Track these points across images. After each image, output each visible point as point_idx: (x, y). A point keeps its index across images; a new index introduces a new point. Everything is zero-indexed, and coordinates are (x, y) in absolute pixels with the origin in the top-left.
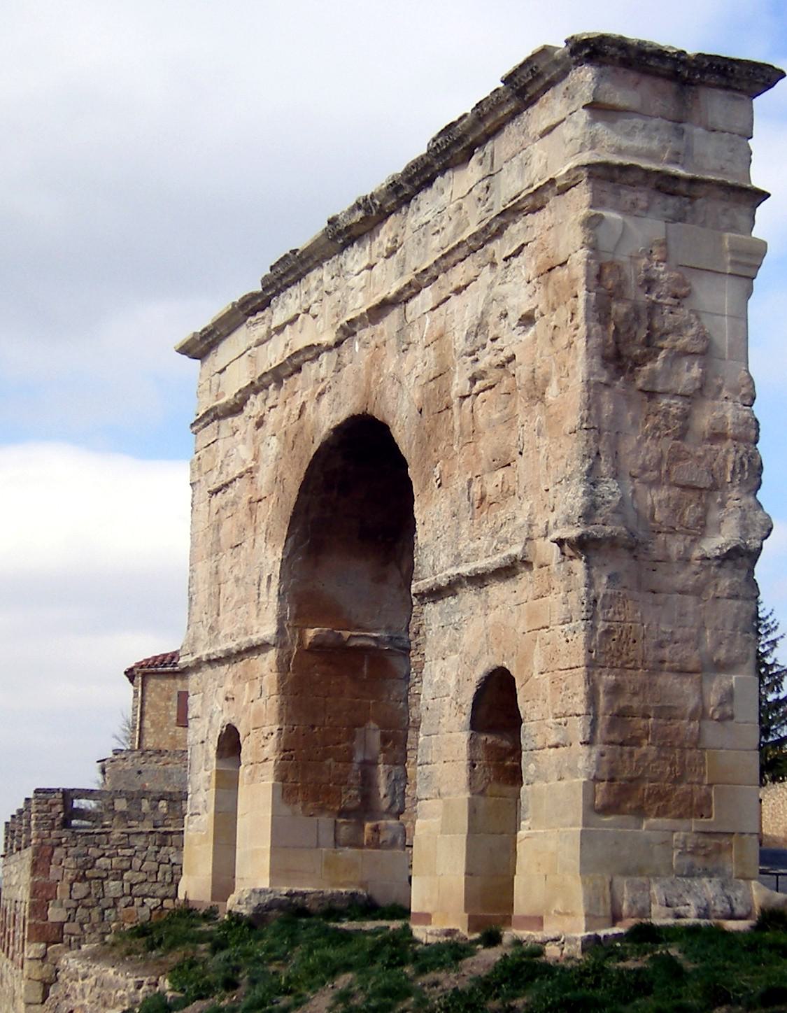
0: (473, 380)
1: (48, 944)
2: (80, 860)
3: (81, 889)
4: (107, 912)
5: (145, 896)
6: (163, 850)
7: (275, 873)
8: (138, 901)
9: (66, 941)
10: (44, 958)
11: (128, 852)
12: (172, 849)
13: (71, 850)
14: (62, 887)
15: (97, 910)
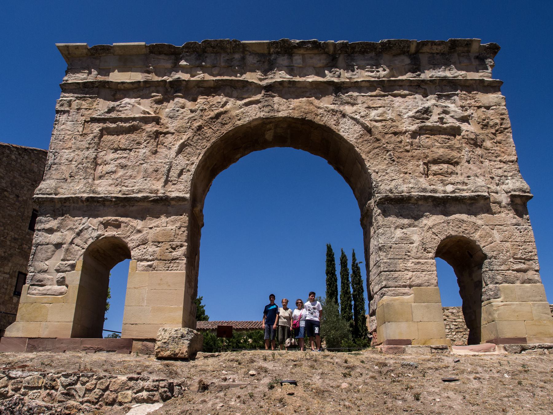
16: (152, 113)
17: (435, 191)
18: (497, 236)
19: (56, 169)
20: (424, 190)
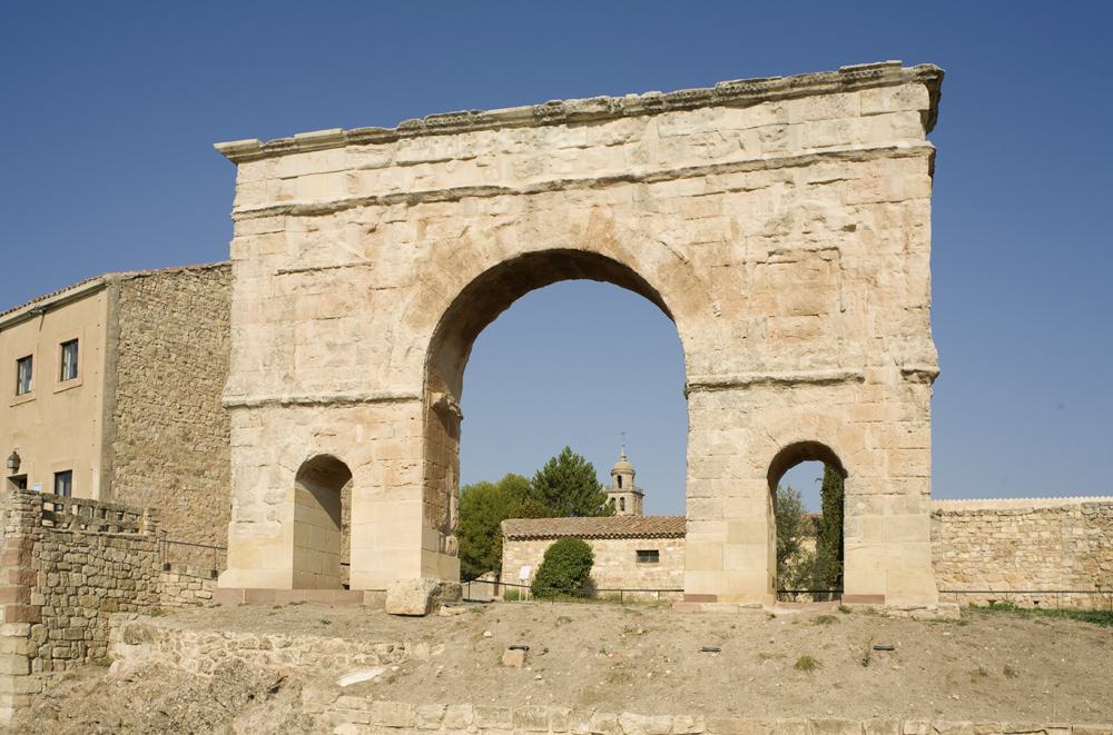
0: (771, 254)
1: (33, 623)
2: (53, 554)
3: (54, 578)
4: (71, 598)
5: (96, 587)
6: (108, 549)
7: (425, 568)
8: (92, 591)
9: (44, 622)
10: (29, 636)
11: (85, 550)
12: (114, 550)
13: (47, 545)
14: (40, 577)
15: (65, 596)
17: (780, 367)
18: (869, 440)
19: (245, 356)
20: (761, 366)
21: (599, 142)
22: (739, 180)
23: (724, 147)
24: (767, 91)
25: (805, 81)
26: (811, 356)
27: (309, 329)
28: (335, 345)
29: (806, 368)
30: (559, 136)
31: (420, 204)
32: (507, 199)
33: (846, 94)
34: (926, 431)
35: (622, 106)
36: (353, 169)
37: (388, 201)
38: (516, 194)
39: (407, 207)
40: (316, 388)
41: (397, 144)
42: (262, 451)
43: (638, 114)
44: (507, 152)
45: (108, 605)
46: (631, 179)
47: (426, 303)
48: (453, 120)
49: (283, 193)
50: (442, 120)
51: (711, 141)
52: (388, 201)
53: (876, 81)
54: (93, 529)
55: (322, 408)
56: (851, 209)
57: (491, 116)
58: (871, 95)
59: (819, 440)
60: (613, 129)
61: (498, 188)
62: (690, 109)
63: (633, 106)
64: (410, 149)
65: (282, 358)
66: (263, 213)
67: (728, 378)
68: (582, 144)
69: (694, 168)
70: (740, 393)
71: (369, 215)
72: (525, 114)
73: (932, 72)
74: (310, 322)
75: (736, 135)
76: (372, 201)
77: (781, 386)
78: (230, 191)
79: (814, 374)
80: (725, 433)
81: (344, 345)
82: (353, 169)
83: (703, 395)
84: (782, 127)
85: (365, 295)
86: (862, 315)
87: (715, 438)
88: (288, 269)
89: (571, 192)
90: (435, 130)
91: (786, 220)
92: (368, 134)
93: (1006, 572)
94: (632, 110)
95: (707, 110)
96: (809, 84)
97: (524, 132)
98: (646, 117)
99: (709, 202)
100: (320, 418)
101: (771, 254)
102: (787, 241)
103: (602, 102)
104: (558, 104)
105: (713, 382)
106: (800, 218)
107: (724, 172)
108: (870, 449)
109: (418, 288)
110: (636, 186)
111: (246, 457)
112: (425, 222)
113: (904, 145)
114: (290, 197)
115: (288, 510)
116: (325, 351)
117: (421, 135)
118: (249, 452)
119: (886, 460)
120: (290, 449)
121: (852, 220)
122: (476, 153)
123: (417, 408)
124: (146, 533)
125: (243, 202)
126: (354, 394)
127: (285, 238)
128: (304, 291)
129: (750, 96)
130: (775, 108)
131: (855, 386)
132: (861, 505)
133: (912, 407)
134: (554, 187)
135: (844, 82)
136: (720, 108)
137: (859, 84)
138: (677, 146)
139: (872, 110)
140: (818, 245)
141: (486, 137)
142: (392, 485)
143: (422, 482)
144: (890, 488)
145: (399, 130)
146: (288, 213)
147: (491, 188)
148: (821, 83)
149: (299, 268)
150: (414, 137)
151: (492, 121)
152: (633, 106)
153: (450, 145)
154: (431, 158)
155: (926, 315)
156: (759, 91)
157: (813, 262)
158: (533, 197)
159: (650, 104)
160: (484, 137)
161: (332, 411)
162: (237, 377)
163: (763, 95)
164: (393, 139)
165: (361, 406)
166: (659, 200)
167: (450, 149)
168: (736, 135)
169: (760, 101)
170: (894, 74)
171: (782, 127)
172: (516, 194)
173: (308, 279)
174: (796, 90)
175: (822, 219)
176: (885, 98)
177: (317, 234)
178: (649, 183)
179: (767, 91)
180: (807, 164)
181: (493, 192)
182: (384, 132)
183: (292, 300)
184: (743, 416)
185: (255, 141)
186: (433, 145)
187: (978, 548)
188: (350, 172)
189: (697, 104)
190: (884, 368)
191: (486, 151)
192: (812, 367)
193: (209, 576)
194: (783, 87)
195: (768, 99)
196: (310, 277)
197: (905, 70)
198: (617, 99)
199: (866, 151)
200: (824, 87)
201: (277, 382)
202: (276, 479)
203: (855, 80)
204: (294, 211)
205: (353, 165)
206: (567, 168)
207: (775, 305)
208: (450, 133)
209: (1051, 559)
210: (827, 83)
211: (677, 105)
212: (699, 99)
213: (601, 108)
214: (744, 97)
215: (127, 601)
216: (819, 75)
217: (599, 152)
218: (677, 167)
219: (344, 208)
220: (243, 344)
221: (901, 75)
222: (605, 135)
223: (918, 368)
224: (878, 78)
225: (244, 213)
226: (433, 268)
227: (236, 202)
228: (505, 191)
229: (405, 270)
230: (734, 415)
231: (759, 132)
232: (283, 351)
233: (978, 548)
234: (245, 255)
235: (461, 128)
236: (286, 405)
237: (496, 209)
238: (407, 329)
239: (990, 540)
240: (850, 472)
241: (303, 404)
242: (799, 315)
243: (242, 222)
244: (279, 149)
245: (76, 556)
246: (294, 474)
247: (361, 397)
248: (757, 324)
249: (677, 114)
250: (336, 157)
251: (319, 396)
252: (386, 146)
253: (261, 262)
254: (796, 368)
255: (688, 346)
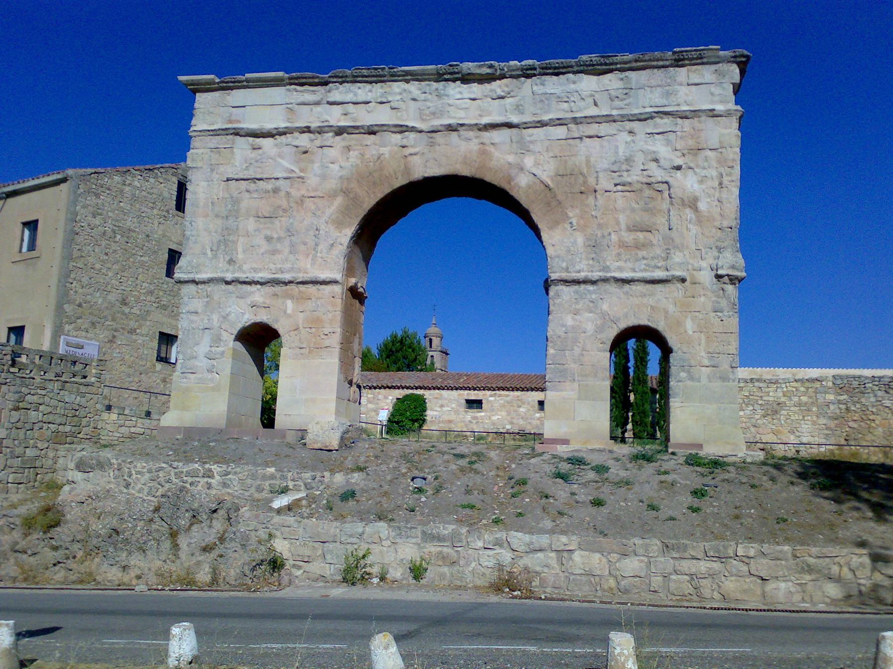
0: (616, 185)
2: (17, 396)
6: (62, 393)
7: (338, 413)
9: (4, 452)
11: (43, 392)
12: (66, 393)
13: (12, 388)
15: (23, 431)
16: (297, 170)
17: (620, 269)
18: (689, 326)
19: (196, 242)
21: (486, 96)
22: (593, 129)
23: (582, 104)
24: (616, 64)
25: (647, 57)
26: (645, 262)
27: (251, 225)
28: (272, 238)
29: (641, 271)
30: (456, 90)
31: (345, 135)
32: (412, 135)
33: (677, 69)
34: (735, 320)
35: (506, 70)
36: (291, 104)
37: (320, 131)
38: (421, 132)
39: (333, 137)
40: (255, 270)
41: (328, 87)
42: (206, 318)
43: (517, 77)
44: (414, 99)
45: (58, 439)
46: (509, 125)
47: (345, 211)
48: (374, 73)
49: (233, 118)
50: (365, 72)
51: (572, 99)
52: (320, 131)
53: (700, 61)
54: (50, 375)
55: (259, 286)
56: (679, 153)
57: (404, 71)
58: (696, 70)
59: (650, 324)
60: (497, 87)
61: (407, 126)
62: (557, 74)
63: (514, 70)
64: (338, 92)
65: (226, 245)
66: (215, 133)
67: (582, 275)
68: (473, 96)
69: (559, 119)
70: (591, 288)
71: (303, 140)
72: (431, 72)
73: (743, 56)
74: (252, 219)
75: (592, 96)
76: (307, 130)
77: (620, 283)
78: (188, 113)
79: (648, 275)
80: (578, 317)
81: (279, 239)
82: (291, 104)
83: (562, 288)
84: (627, 91)
85: (299, 201)
86: (685, 232)
87: (569, 321)
88: (236, 177)
89: (463, 132)
90: (359, 79)
91: (629, 160)
92: (306, 78)
93: (774, 427)
94: (513, 73)
95: (571, 75)
96: (650, 60)
97: (429, 85)
98: (523, 79)
99: (570, 145)
100: (258, 295)
101: (616, 185)
102: (629, 176)
103: (491, 67)
104: (457, 65)
105: (569, 279)
106: (640, 158)
107: (581, 123)
108: (690, 332)
109: (339, 201)
110: (514, 130)
111: (192, 322)
112: (348, 148)
113: (720, 108)
114: (239, 122)
115: (226, 366)
116: (263, 243)
117: (348, 82)
118: (193, 317)
119: (703, 341)
120: (230, 318)
121: (679, 162)
122: (390, 99)
123: (337, 289)
124: (93, 379)
125: (199, 124)
126: (287, 277)
127: (233, 153)
128: (247, 195)
129: (604, 67)
130: (622, 76)
131: (679, 285)
132: (683, 375)
133: (724, 303)
134: (451, 128)
135: (675, 60)
136: (580, 75)
137: (687, 62)
138: (546, 102)
139: (697, 81)
140: (653, 180)
141: (399, 87)
142: (318, 348)
143: (339, 346)
144: (706, 362)
145: (330, 77)
146: (237, 134)
147: (401, 126)
148: (658, 60)
149: (245, 177)
150: (341, 83)
151: (403, 76)
152: (514, 70)
153: (371, 91)
154: (354, 100)
155: (735, 233)
156: (611, 64)
157: (647, 192)
158: (433, 135)
159: (527, 70)
160: (398, 87)
161: (267, 289)
162: (188, 258)
163: (614, 67)
164: (326, 83)
165: (293, 286)
166: (531, 142)
167: (370, 94)
168: (592, 96)
169: (611, 71)
170: (713, 56)
171: (627, 91)
172: (421, 132)
173: (252, 186)
174: (639, 64)
175: (656, 160)
176: (706, 73)
177: (260, 151)
178: (525, 128)
179: (616, 64)
180: (645, 120)
181: (402, 129)
182: (318, 77)
183: (236, 202)
184: (591, 305)
185: (212, 76)
186: (356, 90)
187: (751, 408)
188: (288, 106)
189: (564, 71)
190: (702, 273)
191: (398, 97)
192: (645, 270)
193: (143, 415)
194: (630, 62)
195: (616, 70)
196: (253, 185)
197: (722, 53)
198: (503, 64)
199: (691, 111)
200: (661, 63)
201: (222, 264)
202: (217, 340)
203: (683, 60)
204: (242, 133)
205: (292, 101)
206: (462, 114)
207: (618, 223)
208: (371, 83)
209: (809, 418)
210: (662, 60)
211: (548, 71)
212: (564, 67)
213: (489, 71)
214: (599, 67)
215: (74, 435)
216: (657, 54)
217: (488, 103)
218: (546, 118)
219: (284, 133)
220: (194, 233)
221: (718, 57)
222: (491, 91)
223: (730, 274)
224: (701, 58)
225: (200, 131)
226: (354, 185)
227: (193, 122)
228: (413, 129)
229: (332, 184)
230: (584, 303)
231: (610, 94)
232: (229, 240)
233: (751, 408)
234: (199, 164)
235: (379, 79)
236: (228, 283)
237: (405, 142)
238: (331, 228)
239: (760, 402)
240: (675, 348)
241: (245, 283)
242: (637, 231)
243: (197, 139)
244: (231, 84)
245: (35, 397)
246: (233, 337)
247: (292, 279)
248: (603, 236)
249: (547, 78)
250: (277, 94)
251: (258, 276)
252: (319, 88)
253: (212, 170)
254: (634, 270)
255: (550, 251)
